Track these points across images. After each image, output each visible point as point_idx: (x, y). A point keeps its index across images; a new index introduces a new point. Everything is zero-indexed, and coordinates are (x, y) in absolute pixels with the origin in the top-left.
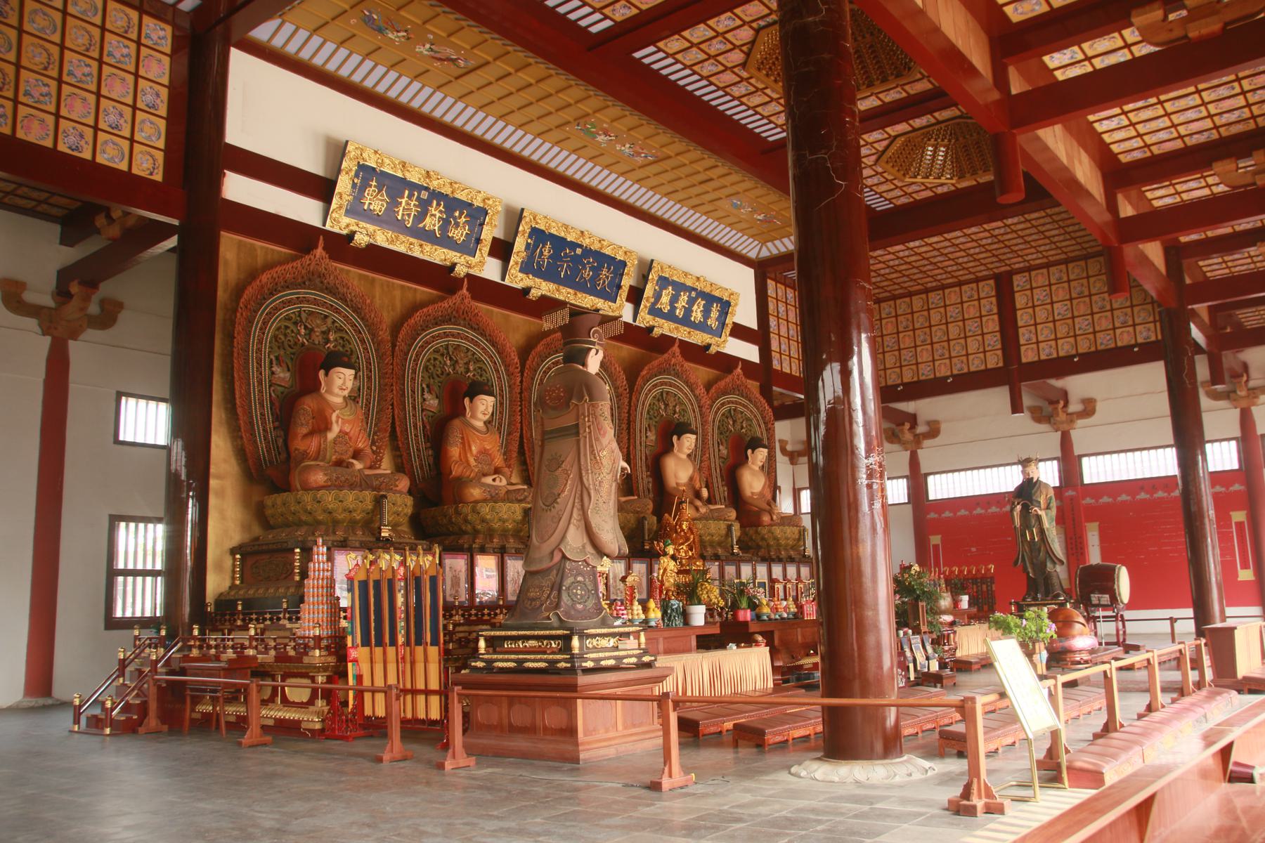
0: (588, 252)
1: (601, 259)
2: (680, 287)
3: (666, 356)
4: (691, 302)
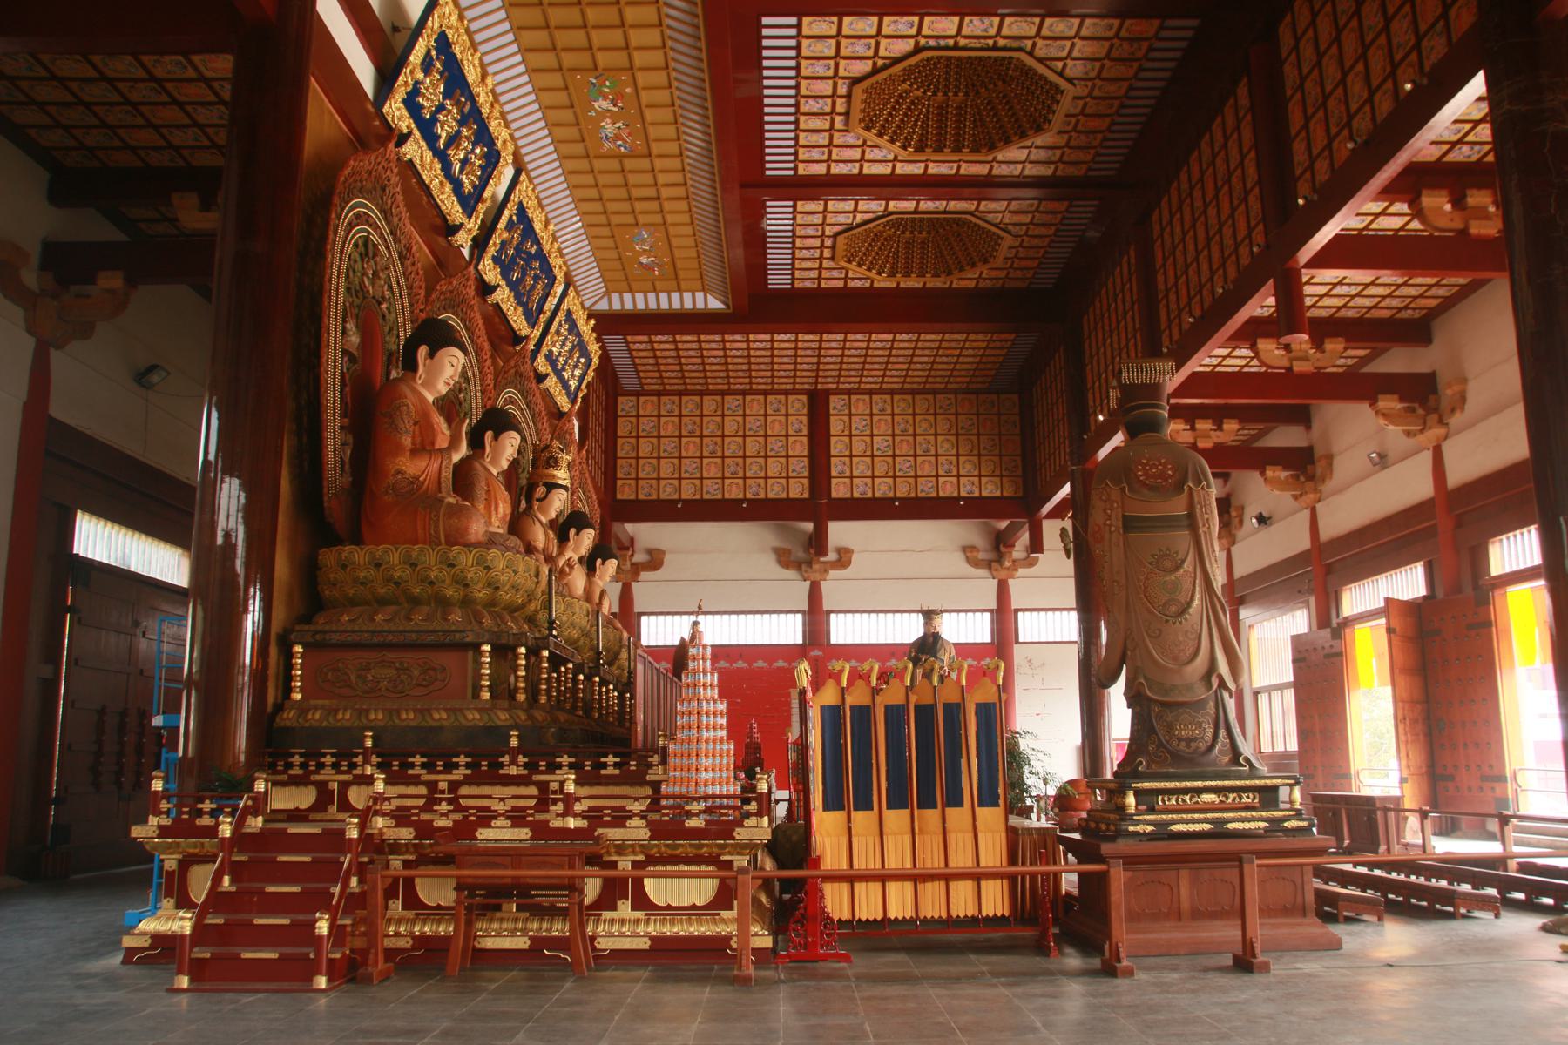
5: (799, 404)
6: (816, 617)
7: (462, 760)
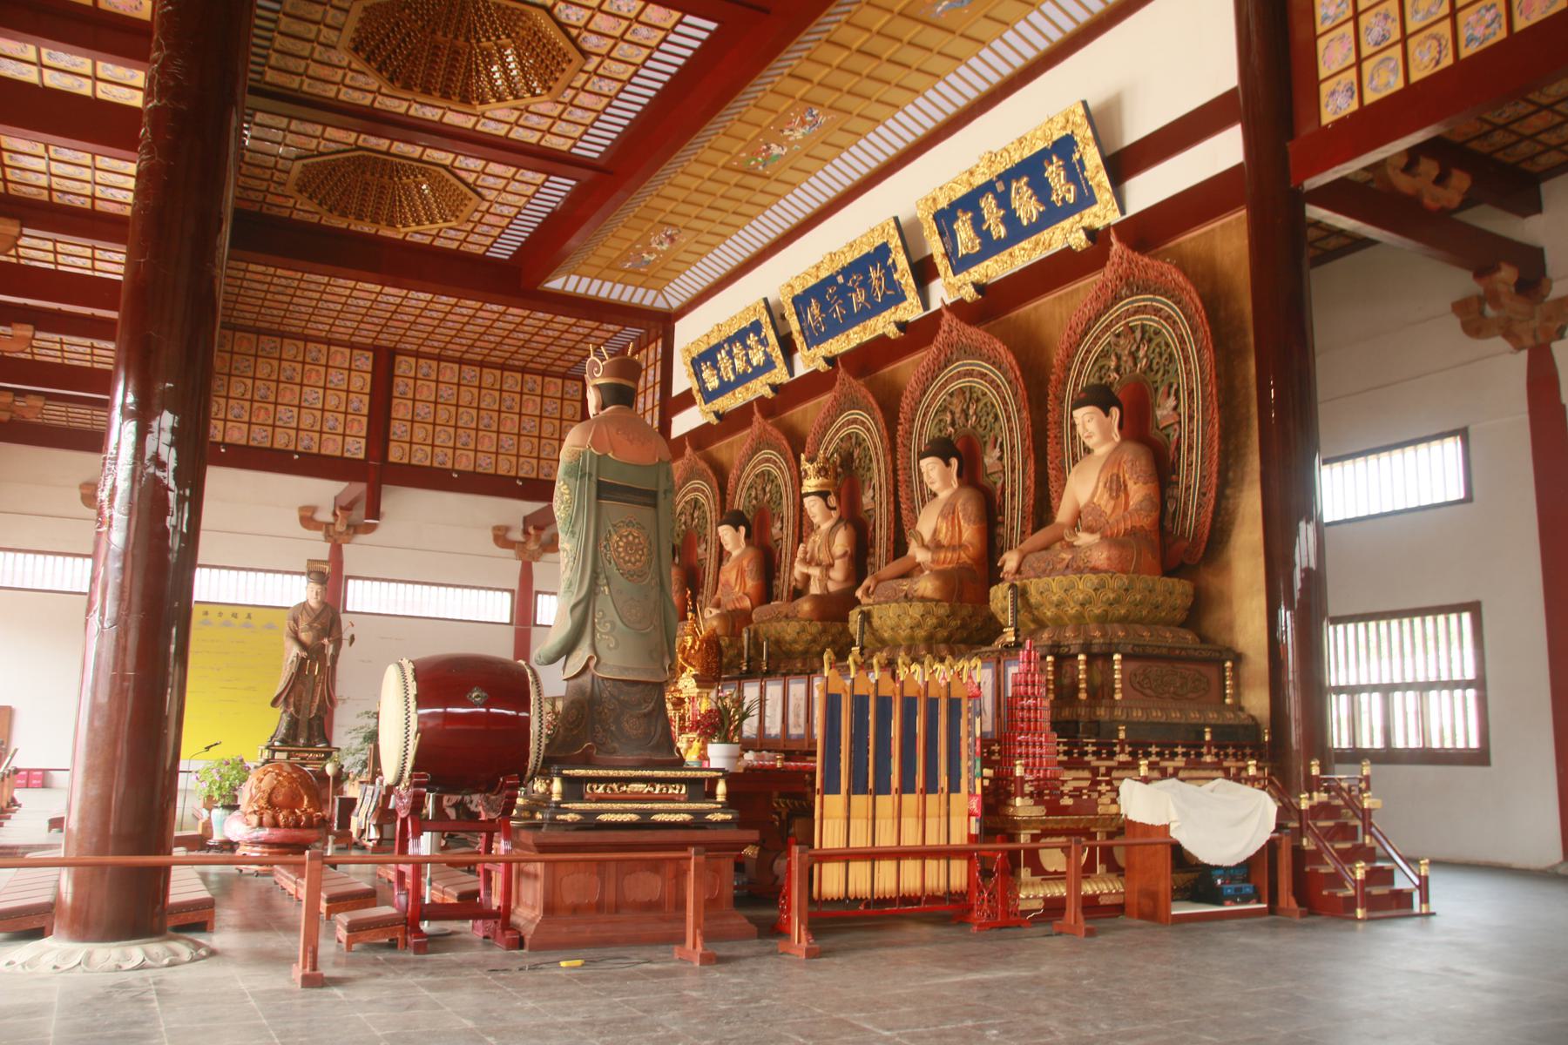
0: (847, 271)
1: (860, 266)
2: (970, 202)
3: (941, 336)
4: (1004, 201)
5: (365, 362)
6: (331, 578)
7: (1180, 750)
